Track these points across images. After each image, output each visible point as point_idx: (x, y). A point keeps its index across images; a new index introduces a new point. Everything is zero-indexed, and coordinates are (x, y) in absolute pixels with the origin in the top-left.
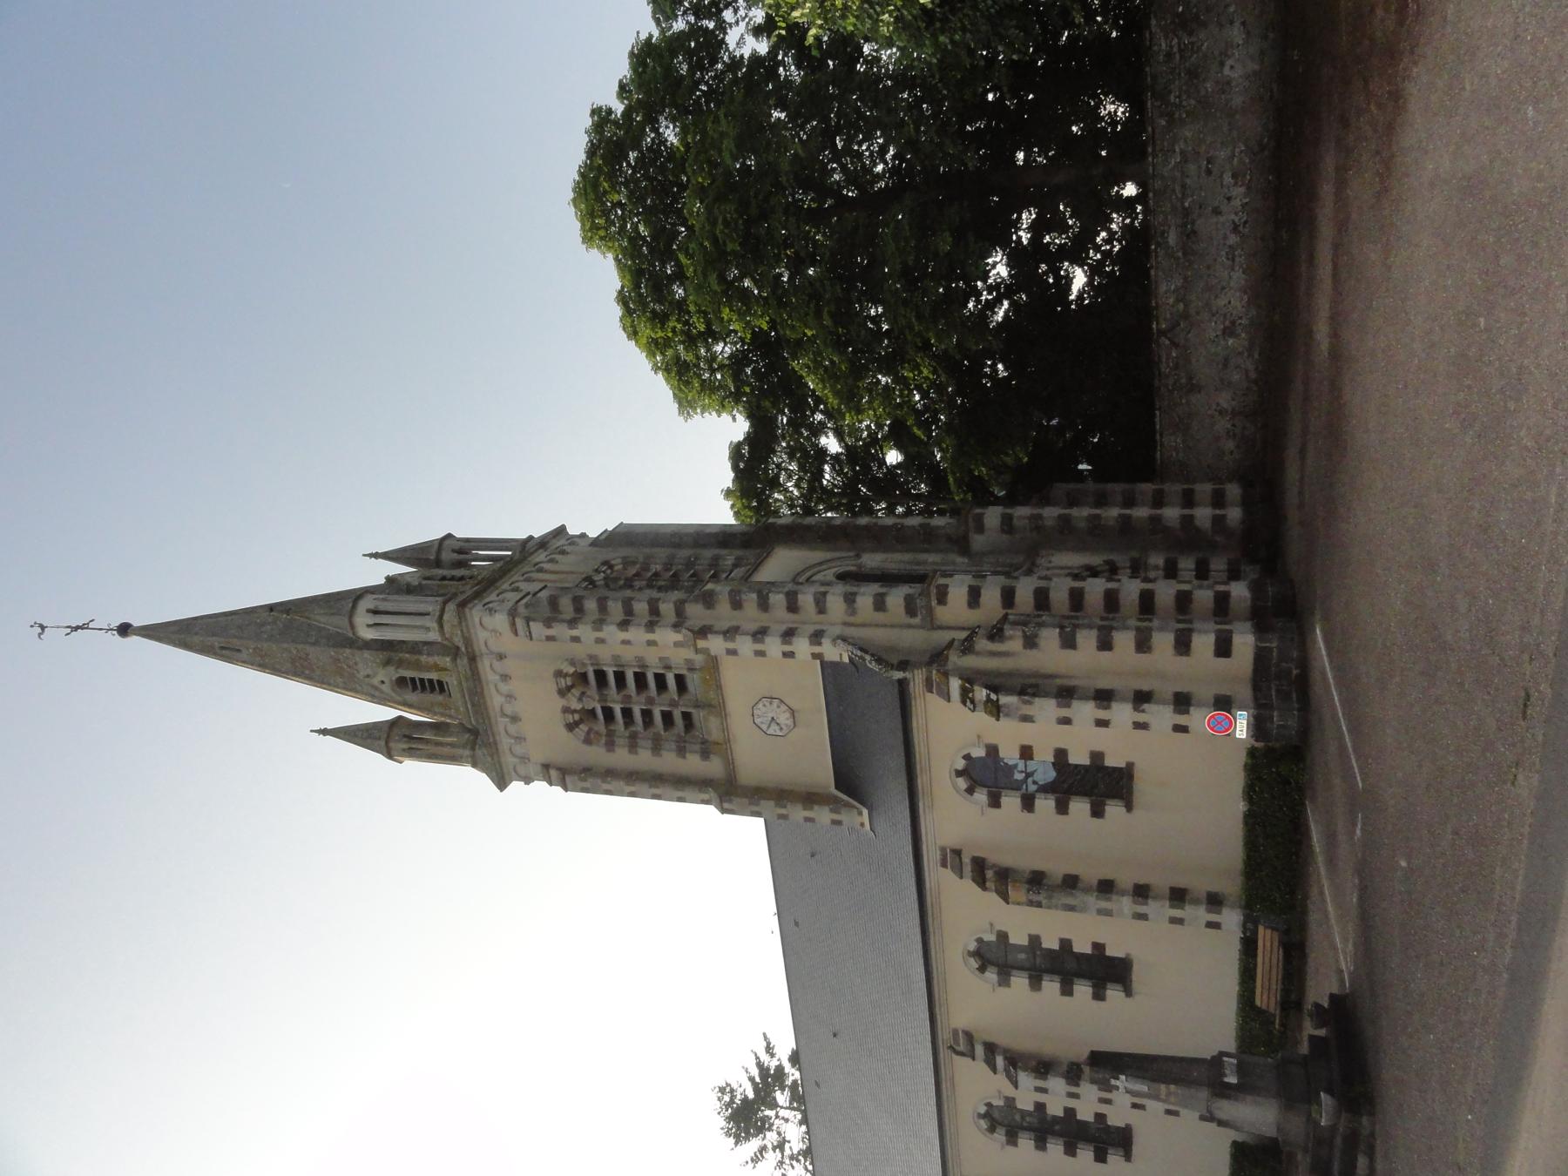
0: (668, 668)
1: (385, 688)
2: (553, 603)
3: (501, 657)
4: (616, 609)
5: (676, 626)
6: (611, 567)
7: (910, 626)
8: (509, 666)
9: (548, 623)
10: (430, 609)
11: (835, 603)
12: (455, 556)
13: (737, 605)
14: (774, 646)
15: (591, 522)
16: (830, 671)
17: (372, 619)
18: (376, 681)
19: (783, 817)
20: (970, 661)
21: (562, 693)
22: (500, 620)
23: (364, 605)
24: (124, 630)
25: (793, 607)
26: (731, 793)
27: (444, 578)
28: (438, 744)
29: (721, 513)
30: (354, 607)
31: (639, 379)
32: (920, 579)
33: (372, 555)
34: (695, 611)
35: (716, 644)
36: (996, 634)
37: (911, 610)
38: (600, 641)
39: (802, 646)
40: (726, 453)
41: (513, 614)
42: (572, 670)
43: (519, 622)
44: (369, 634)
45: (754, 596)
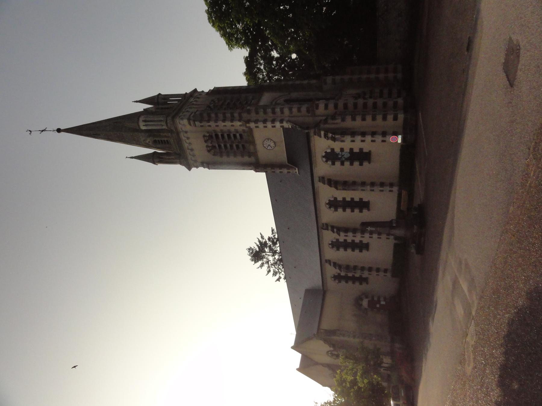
0: (237, 132)
1: (150, 144)
2: (201, 114)
3: (186, 132)
4: (221, 116)
5: (240, 120)
6: (214, 102)
7: (308, 116)
8: (189, 135)
9: (201, 122)
10: (163, 119)
11: (286, 111)
12: (163, 101)
13: (257, 113)
14: (269, 125)
15: (205, 87)
16: (286, 131)
17: (144, 124)
18: (147, 142)
19: (274, 172)
20: (327, 126)
21: (206, 141)
22: (185, 122)
23: (141, 119)
24: (59, 130)
25: (274, 112)
26: (257, 167)
27: (162, 108)
28: (169, 159)
29: (243, 82)
30: (138, 120)
31: (214, 38)
32: (309, 100)
33: (135, 102)
34: (245, 115)
35: (252, 125)
36: (333, 117)
37: (308, 111)
38: (217, 126)
39: (278, 124)
40: (243, 60)
41: (189, 119)
42: (208, 135)
43: (192, 122)
44: (143, 128)
45: (262, 110)
